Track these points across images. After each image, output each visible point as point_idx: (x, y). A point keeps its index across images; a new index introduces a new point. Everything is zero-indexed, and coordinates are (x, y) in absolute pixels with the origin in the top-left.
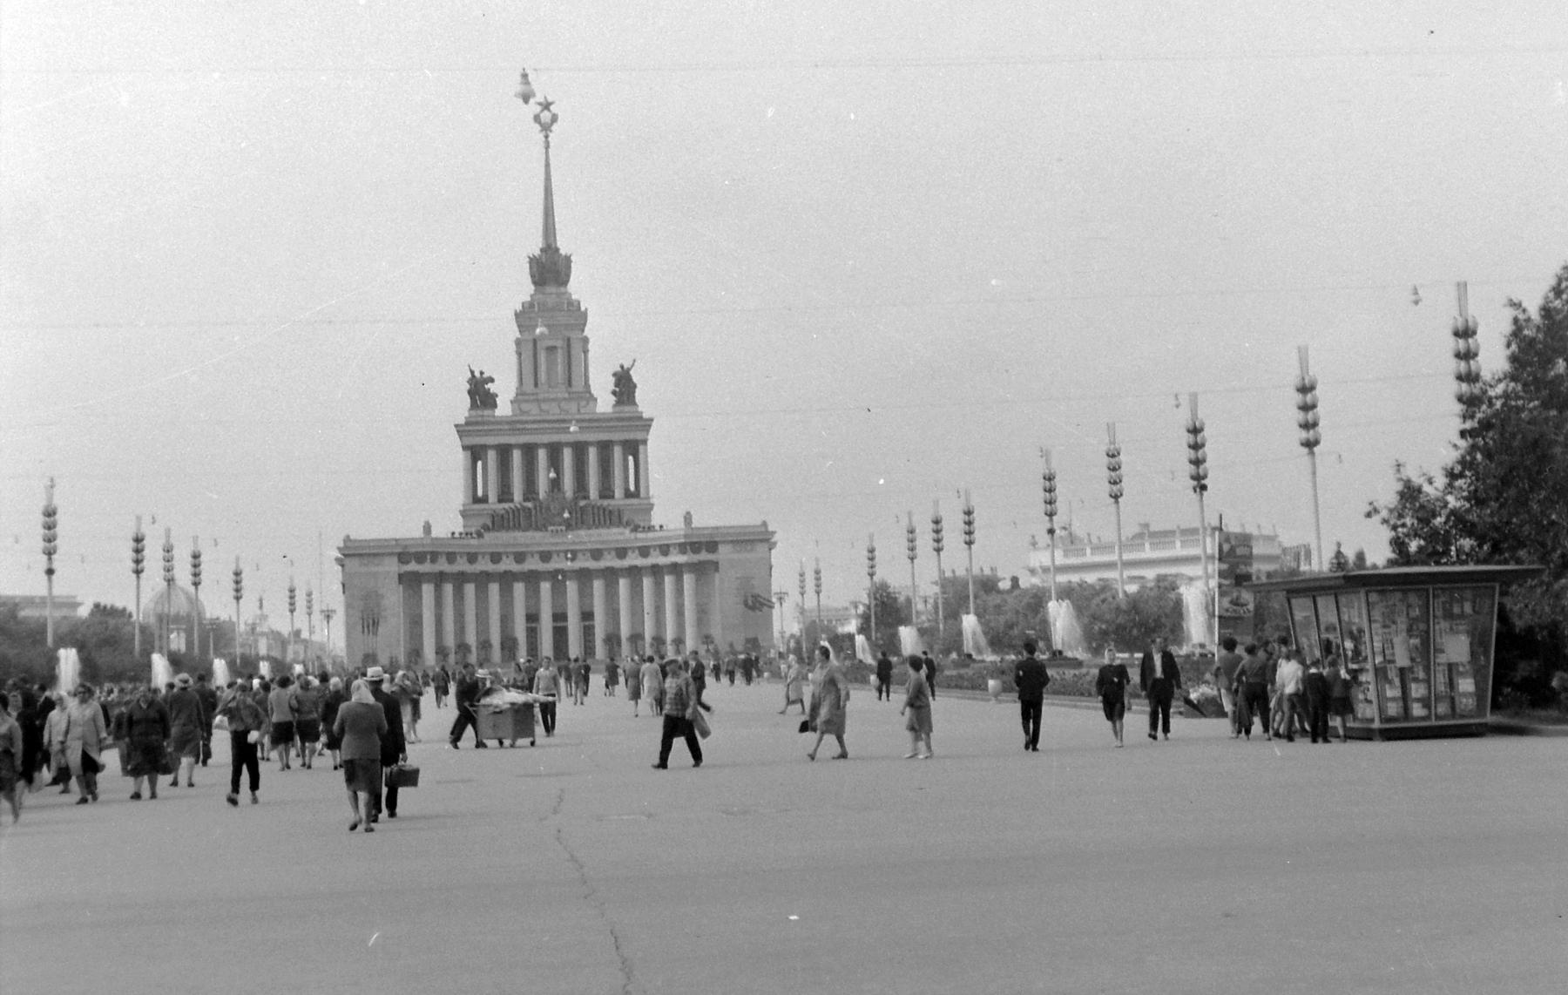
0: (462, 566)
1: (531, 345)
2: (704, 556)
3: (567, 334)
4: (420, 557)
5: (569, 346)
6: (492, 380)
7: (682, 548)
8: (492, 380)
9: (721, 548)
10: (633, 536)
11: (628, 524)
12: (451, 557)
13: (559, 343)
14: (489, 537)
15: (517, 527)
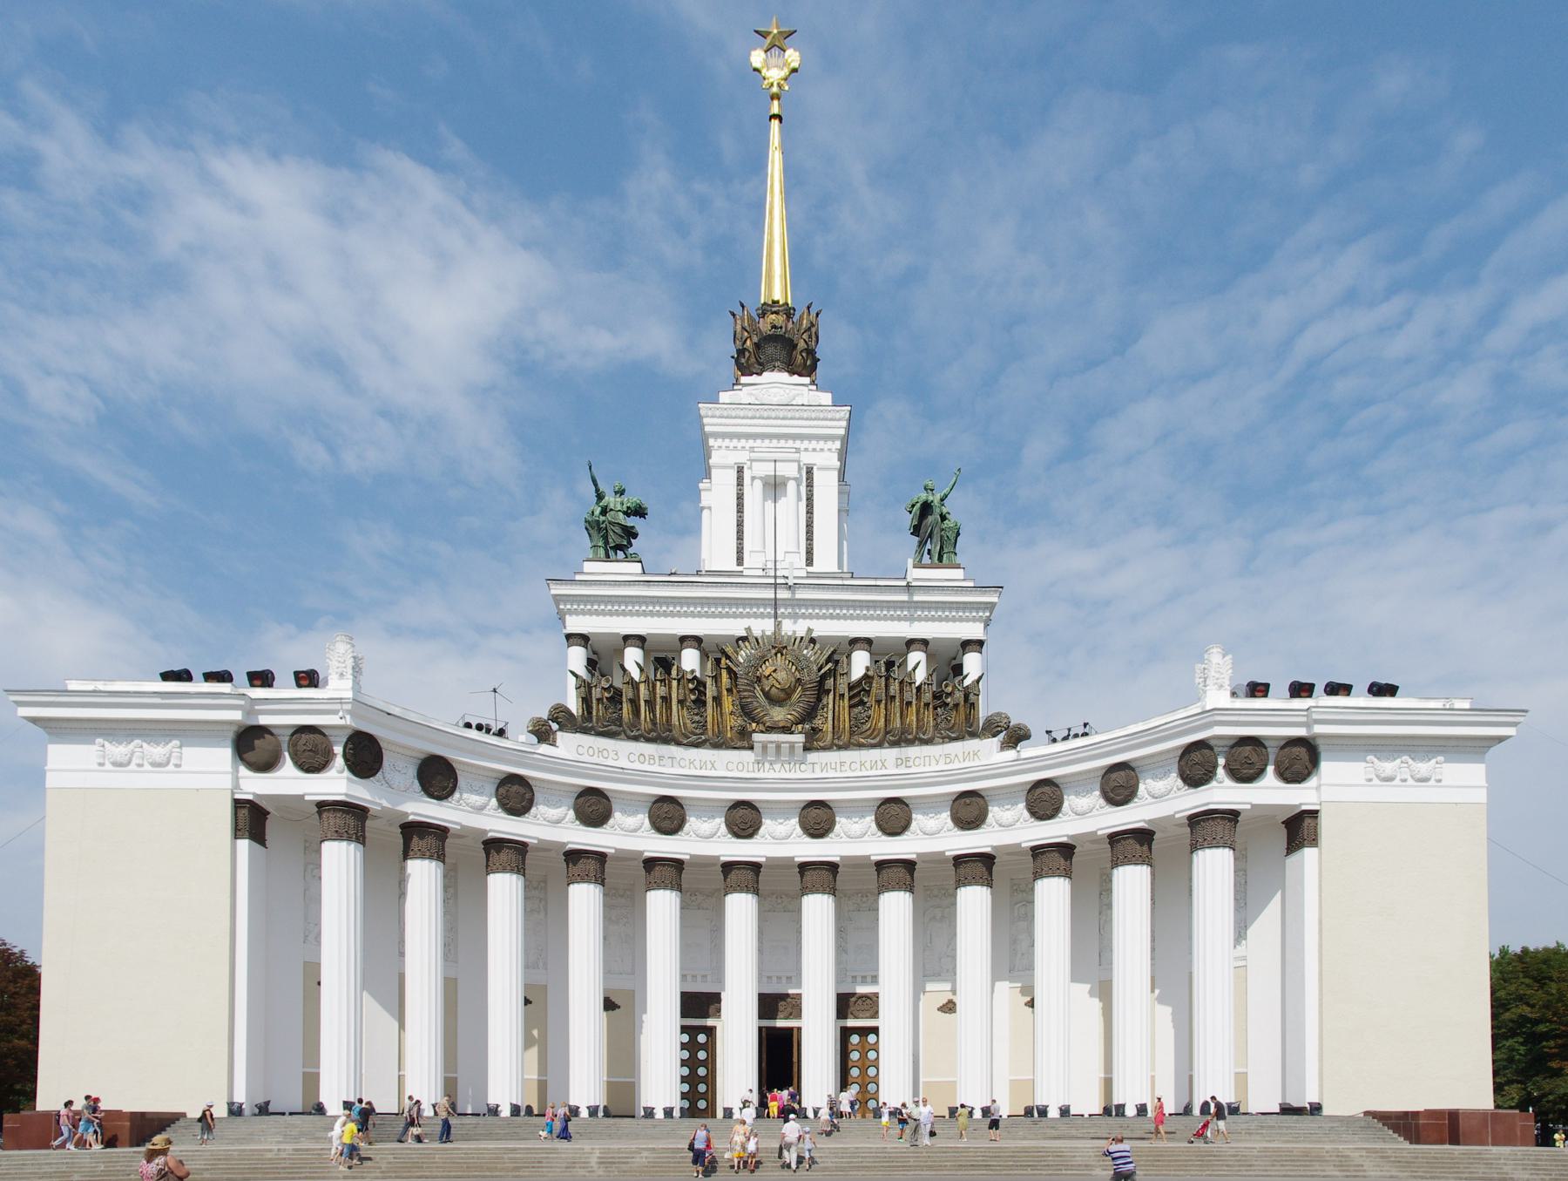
0: (472, 813)
1: (733, 474)
2: (1270, 792)
3: (807, 458)
4: (310, 749)
5: (810, 485)
6: (639, 512)
7: (1195, 764)
8: (639, 512)
9: (1328, 768)
10: (1011, 754)
11: (993, 727)
12: (437, 776)
13: (788, 470)
14: (569, 745)
15: (662, 735)
